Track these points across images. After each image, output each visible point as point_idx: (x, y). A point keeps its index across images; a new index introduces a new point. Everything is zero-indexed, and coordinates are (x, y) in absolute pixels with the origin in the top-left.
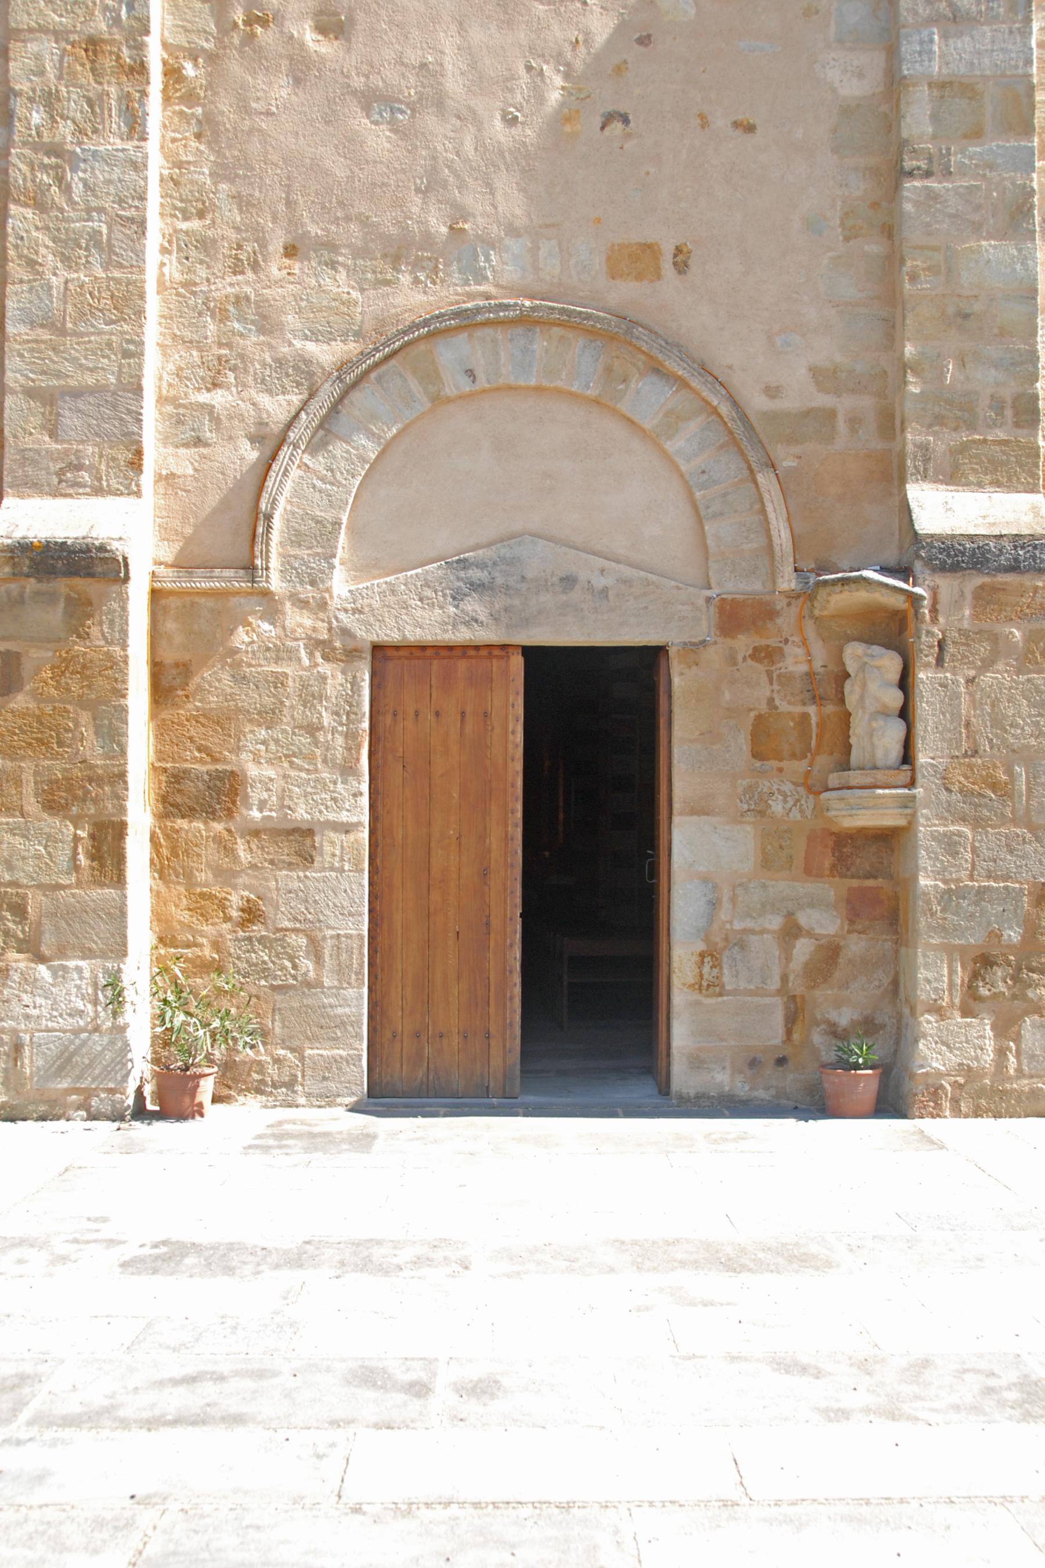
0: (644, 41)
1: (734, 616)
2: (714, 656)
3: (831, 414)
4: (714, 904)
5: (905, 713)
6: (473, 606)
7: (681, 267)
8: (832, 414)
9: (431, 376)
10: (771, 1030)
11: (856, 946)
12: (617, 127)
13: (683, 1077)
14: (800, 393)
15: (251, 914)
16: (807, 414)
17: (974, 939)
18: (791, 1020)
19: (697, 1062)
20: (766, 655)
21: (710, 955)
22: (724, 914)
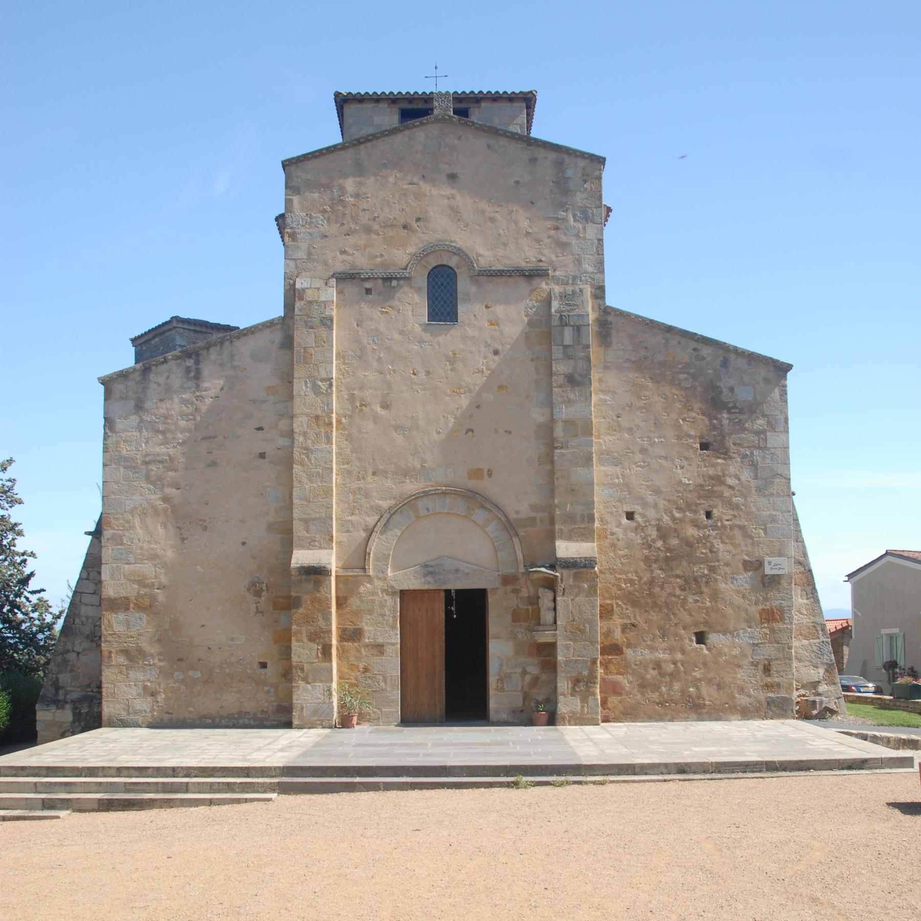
0: (478, 407)
1: (507, 580)
3: (535, 519)
4: (501, 665)
5: (555, 609)
6: (429, 579)
7: (490, 475)
10: (519, 702)
11: (544, 677)
12: (470, 433)
13: (492, 715)
15: (366, 670)
16: (528, 518)
17: (574, 674)
18: (525, 699)
19: (497, 711)
20: (516, 591)
21: (500, 680)
22: (504, 668)
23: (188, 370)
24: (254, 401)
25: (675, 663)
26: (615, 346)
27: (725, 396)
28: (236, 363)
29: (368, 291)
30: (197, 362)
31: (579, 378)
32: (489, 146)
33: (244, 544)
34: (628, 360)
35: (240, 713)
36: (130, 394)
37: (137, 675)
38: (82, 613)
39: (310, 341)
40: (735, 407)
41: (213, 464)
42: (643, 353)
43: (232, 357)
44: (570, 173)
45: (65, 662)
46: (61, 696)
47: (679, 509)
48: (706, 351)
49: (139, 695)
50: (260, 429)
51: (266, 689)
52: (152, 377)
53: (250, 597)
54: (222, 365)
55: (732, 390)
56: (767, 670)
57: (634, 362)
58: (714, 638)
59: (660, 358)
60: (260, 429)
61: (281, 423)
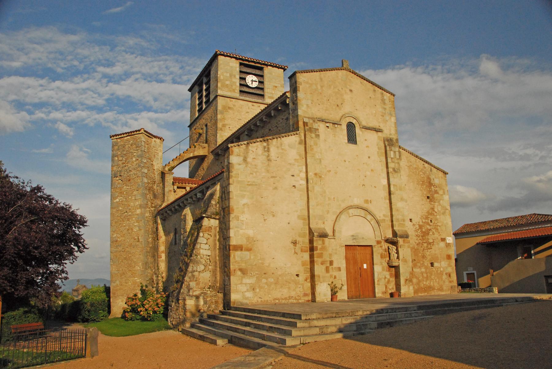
1: (378, 242)
2: (377, 247)
6: (354, 241)
9: (348, 214)
10: (384, 289)
11: (391, 279)
14: (382, 218)
18: (386, 288)
19: (378, 293)
20: (381, 247)
23: (265, 147)
24: (290, 164)
25: (427, 273)
27: (432, 182)
29: (327, 127)
30: (268, 145)
35: (289, 297)
36: (241, 154)
37: (247, 280)
39: (312, 143)
41: (276, 188)
42: (410, 164)
43: (281, 144)
44: (385, 97)
45: (193, 276)
48: (426, 165)
49: (247, 290)
50: (293, 176)
51: (299, 286)
52: (250, 148)
53: (292, 246)
54: (278, 147)
56: (450, 276)
58: (436, 264)
59: (415, 166)
60: (293, 176)
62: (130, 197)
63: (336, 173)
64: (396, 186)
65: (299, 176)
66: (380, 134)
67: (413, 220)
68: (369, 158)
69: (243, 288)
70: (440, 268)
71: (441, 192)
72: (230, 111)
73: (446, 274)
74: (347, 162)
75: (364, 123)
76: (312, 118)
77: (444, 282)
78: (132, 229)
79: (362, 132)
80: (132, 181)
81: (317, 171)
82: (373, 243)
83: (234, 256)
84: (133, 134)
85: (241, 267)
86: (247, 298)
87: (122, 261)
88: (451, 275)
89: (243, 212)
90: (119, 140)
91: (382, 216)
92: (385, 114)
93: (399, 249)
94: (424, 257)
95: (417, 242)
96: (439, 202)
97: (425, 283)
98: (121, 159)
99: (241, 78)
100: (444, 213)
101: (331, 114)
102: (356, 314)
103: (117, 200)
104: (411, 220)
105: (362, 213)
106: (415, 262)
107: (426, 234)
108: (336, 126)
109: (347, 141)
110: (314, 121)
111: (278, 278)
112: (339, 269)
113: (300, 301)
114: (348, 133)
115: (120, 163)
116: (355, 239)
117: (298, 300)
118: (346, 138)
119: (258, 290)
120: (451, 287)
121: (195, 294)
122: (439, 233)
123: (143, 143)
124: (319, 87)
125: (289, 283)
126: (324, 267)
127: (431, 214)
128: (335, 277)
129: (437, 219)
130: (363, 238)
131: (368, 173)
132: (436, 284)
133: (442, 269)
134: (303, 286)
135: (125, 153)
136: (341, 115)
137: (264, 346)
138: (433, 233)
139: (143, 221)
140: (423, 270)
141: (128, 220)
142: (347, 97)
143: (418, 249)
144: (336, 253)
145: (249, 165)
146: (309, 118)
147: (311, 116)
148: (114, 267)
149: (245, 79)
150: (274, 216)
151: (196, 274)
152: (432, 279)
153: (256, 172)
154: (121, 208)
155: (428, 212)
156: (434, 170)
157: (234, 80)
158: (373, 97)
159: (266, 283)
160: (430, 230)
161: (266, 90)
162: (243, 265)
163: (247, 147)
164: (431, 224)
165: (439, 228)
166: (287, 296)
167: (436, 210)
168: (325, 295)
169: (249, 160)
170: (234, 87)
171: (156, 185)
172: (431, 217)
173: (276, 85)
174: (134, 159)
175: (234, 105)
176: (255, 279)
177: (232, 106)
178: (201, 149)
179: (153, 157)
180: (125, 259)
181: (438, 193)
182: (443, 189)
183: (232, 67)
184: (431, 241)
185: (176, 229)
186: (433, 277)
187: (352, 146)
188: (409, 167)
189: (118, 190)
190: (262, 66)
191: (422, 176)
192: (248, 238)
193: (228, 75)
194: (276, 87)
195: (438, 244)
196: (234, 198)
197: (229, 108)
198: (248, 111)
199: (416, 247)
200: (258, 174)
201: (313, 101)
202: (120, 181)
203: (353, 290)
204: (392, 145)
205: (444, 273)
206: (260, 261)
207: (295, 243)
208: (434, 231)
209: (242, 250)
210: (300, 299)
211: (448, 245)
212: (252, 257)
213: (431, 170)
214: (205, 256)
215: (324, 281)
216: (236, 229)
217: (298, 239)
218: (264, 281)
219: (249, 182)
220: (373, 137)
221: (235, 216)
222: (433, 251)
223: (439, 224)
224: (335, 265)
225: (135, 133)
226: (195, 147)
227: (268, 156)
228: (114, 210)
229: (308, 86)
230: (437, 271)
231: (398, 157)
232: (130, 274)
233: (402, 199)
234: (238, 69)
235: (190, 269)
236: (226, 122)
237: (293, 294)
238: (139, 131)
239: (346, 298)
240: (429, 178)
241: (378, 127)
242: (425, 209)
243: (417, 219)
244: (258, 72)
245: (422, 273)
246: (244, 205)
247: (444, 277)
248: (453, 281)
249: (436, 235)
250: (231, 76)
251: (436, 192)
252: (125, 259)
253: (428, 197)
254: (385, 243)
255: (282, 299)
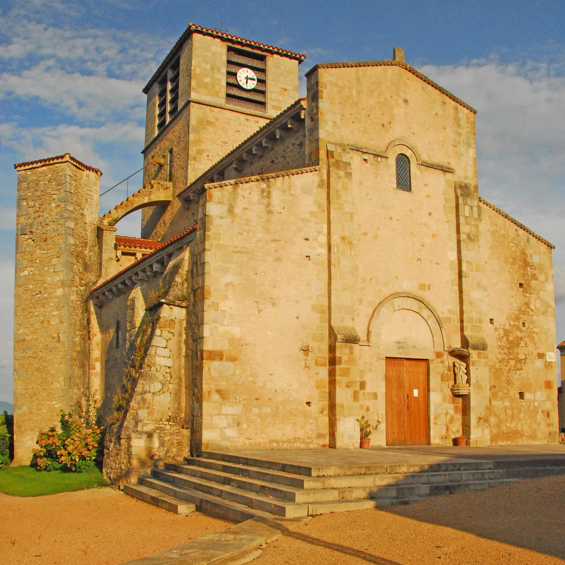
1: (439, 355)
2: (435, 362)
3: (450, 318)
4: (436, 408)
6: (401, 351)
7: (429, 289)
8: (450, 318)
9: (393, 306)
10: (444, 432)
12: (419, 261)
14: (446, 315)
16: (448, 318)
18: (447, 430)
20: (442, 362)
23: (263, 191)
24: (303, 220)
26: (483, 221)
27: (529, 259)
28: (292, 192)
29: (365, 160)
30: (269, 186)
31: (473, 237)
32: (423, 89)
33: (298, 318)
34: (489, 231)
35: (294, 438)
37: (228, 409)
38: (157, 362)
39: (340, 186)
40: (532, 266)
41: (279, 259)
42: (495, 228)
43: (290, 187)
44: (461, 115)
46: (139, 429)
47: (512, 320)
48: (521, 232)
51: (311, 421)
53: (301, 354)
54: (284, 191)
55: (531, 256)
56: (548, 415)
57: (492, 232)
58: (527, 396)
59: (502, 232)
61: (319, 237)
62: (46, 268)
63: (376, 238)
64: (471, 263)
65: (316, 240)
66: (448, 175)
67: (494, 321)
68: (430, 215)
69: (222, 422)
70: (534, 402)
71: (542, 278)
72: (210, 129)
73: (543, 412)
74: (394, 220)
75: (424, 157)
76: (340, 145)
77: (539, 425)
78: (48, 321)
79: (421, 171)
80: (49, 241)
81: (346, 233)
82: (430, 356)
83: (209, 369)
84: (51, 162)
85: (219, 388)
86: (227, 439)
87: (33, 374)
88: (551, 414)
89: (226, 297)
90: (29, 173)
91: (446, 312)
92: (459, 142)
93: (471, 368)
94: (509, 382)
95: (500, 357)
96: (538, 293)
97: (508, 425)
98: (31, 204)
99: (229, 73)
100: (544, 313)
101: (371, 140)
102: (398, 471)
103: (26, 273)
104: (491, 320)
105: (415, 305)
106: (496, 390)
107: (514, 344)
108: (379, 159)
109: (395, 186)
110: (344, 150)
111: (278, 408)
112: (375, 396)
113: (311, 446)
114: (397, 172)
115: (31, 210)
116: (401, 347)
117: (308, 443)
118: (395, 180)
119: (245, 426)
120: (550, 434)
121: (146, 429)
122: (535, 344)
123: (68, 177)
124: (354, 93)
125: (295, 415)
126: (350, 392)
127: (524, 313)
128: (368, 409)
129: (533, 322)
130: (414, 347)
131: (427, 240)
132: (526, 428)
133: (536, 404)
134: (317, 422)
135: (38, 194)
136: (387, 141)
137: (251, 516)
138: (526, 344)
139: (66, 308)
140: (507, 403)
141: (43, 306)
142: (399, 111)
143: (501, 369)
144: (370, 370)
145: (237, 220)
146: (336, 144)
147: (338, 141)
148: (19, 382)
149: (235, 75)
150: (274, 304)
151: (148, 396)
152: (520, 420)
153: (248, 232)
154: (31, 286)
155: (519, 310)
156: (533, 241)
157: (217, 76)
158: (442, 113)
159: (259, 415)
160: (521, 338)
161: (268, 94)
162: (223, 384)
163: (235, 189)
164: (523, 329)
165: (535, 335)
166: (292, 437)
167: (532, 307)
168: (351, 438)
169: (238, 210)
170: (217, 88)
171: (88, 249)
172: (524, 317)
173: (286, 86)
174: (53, 205)
175: (217, 119)
176: (241, 407)
177: (214, 121)
178: (162, 190)
179: (84, 201)
180: (38, 370)
181: (537, 279)
182: (546, 273)
183: (214, 53)
184: (522, 356)
185: (118, 322)
186: (522, 415)
187: (404, 194)
188: (494, 233)
189: (26, 257)
190: (264, 54)
191: (514, 249)
192: (232, 340)
193: (208, 67)
194: (286, 90)
195: (533, 363)
196: (212, 273)
197: (209, 123)
198: (239, 128)
199: (498, 365)
200: (251, 234)
201: (343, 115)
202: (30, 241)
203: (396, 431)
204: (468, 195)
205: (540, 410)
206: (250, 379)
207: (306, 350)
208: (528, 340)
209: (221, 359)
210: (311, 443)
211: (548, 365)
212: (237, 372)
213: (528, 241)
214: (163, 368)
215: (350, 415)
216: (213, 325)
217: (312, 344)
218: (255, 410)
219: (236, 247)
220: (437, 180)
221: (213, 302)
222: (523, 373)
223: (536, 330)
224: (369, 388)
225: (56, 161)
226: (152, 187)
227: (268, 205)
228: (21, 290)
229: (336, 90)
230: (529, 407)
231: (476, 215)
232: (44, 395)
233: (479, 286)
234: (224, 58)
235: (139, 389)
236: (203, 147)
237: (300, 433)
238: (62, 157)
239: (383, 443)
240: (524, 253)
241: (446, 164)
242: (515, 304)
243: (501, 321)
244: (257, 63)
245: (505, 408)
246: (227, 285)
247: (540, 416)
248: (553, 425)
249: (531, 348)
250: (212, 68)
251: (534, 277)
252: (38, 370)
253: (521, 285)
254: (449, 357)
255: (283, 442)
